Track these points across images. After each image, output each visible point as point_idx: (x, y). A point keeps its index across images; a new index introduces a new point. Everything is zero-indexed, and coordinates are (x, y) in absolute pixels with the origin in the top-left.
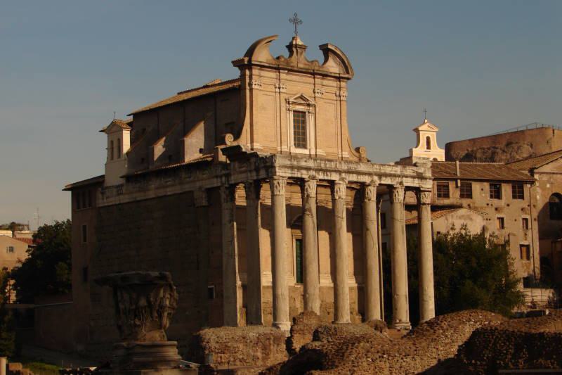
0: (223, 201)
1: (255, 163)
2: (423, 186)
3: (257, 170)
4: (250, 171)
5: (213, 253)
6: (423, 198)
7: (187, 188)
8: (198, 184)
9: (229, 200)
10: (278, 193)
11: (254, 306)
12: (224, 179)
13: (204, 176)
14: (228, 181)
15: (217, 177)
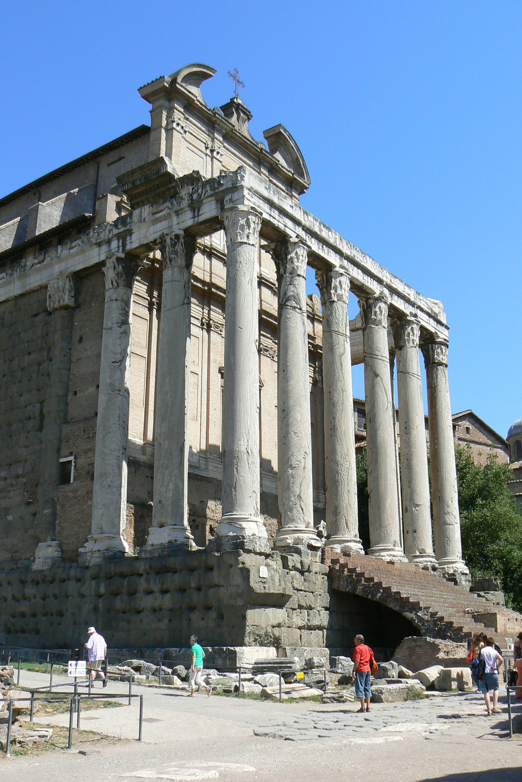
0: (108, 285)
1: (191, 195)
2: (440, 334)
3: (195, 206)
4: (178, 213)
5: (75, 393)
6: (438, 354)
7: (34, 281)
8: (57, 268)
9: (121, 282)
10: (245, 240)
11: (171, 487)
12: (114, 244)
13: (71, 251)
14: (124, 245)
15: (99, 245)
